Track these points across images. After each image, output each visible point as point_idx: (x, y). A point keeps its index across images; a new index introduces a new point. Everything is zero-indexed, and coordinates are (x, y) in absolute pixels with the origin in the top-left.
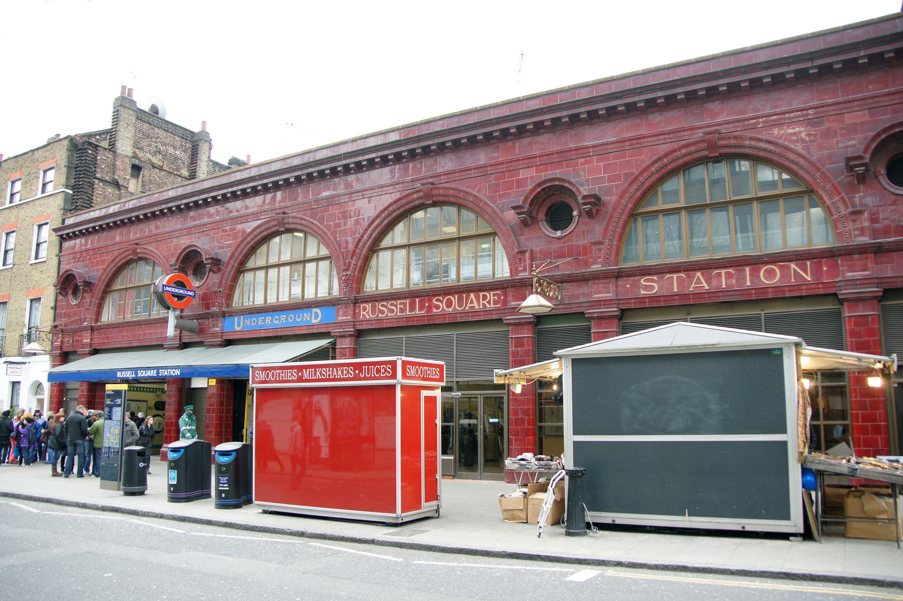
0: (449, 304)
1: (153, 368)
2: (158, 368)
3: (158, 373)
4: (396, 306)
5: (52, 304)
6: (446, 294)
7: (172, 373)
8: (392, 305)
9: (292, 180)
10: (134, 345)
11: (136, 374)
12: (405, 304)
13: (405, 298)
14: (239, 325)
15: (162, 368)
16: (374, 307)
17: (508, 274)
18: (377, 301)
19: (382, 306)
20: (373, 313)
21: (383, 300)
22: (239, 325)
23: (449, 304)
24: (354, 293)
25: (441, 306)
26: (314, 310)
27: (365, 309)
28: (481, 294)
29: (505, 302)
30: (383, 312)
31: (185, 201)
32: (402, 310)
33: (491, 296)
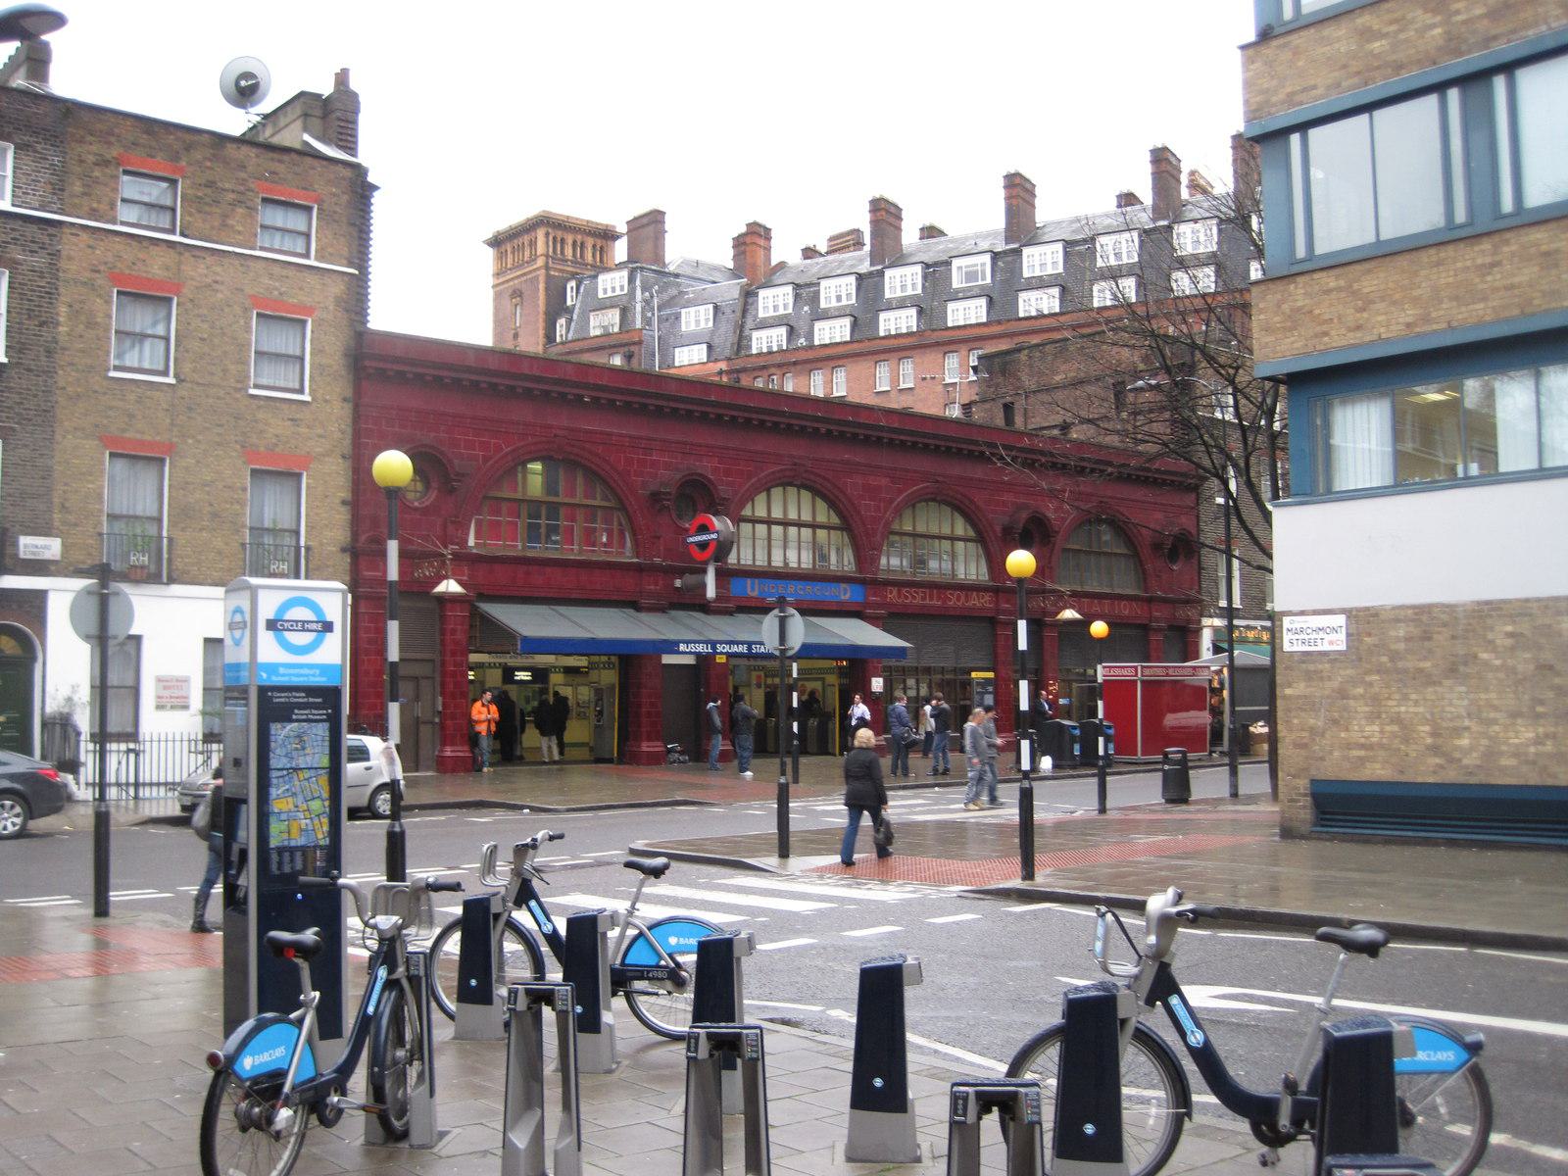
0: (958, 600)
1: (743, 643)
2: (750, 644)
3: (750, 648)
5: (346, 494)
11: (714, 648)
13: (926, 587)
14: (753, 589)
15: (756, 643)
16: (899, 592)
17: (987, 578)
20: (899, 597)
22: (753, 589)
23: (958, 600)
25: (954, 601)
26: (843, 586)
30: (907, 598)
32: (923, 599)
33: (987, 597)
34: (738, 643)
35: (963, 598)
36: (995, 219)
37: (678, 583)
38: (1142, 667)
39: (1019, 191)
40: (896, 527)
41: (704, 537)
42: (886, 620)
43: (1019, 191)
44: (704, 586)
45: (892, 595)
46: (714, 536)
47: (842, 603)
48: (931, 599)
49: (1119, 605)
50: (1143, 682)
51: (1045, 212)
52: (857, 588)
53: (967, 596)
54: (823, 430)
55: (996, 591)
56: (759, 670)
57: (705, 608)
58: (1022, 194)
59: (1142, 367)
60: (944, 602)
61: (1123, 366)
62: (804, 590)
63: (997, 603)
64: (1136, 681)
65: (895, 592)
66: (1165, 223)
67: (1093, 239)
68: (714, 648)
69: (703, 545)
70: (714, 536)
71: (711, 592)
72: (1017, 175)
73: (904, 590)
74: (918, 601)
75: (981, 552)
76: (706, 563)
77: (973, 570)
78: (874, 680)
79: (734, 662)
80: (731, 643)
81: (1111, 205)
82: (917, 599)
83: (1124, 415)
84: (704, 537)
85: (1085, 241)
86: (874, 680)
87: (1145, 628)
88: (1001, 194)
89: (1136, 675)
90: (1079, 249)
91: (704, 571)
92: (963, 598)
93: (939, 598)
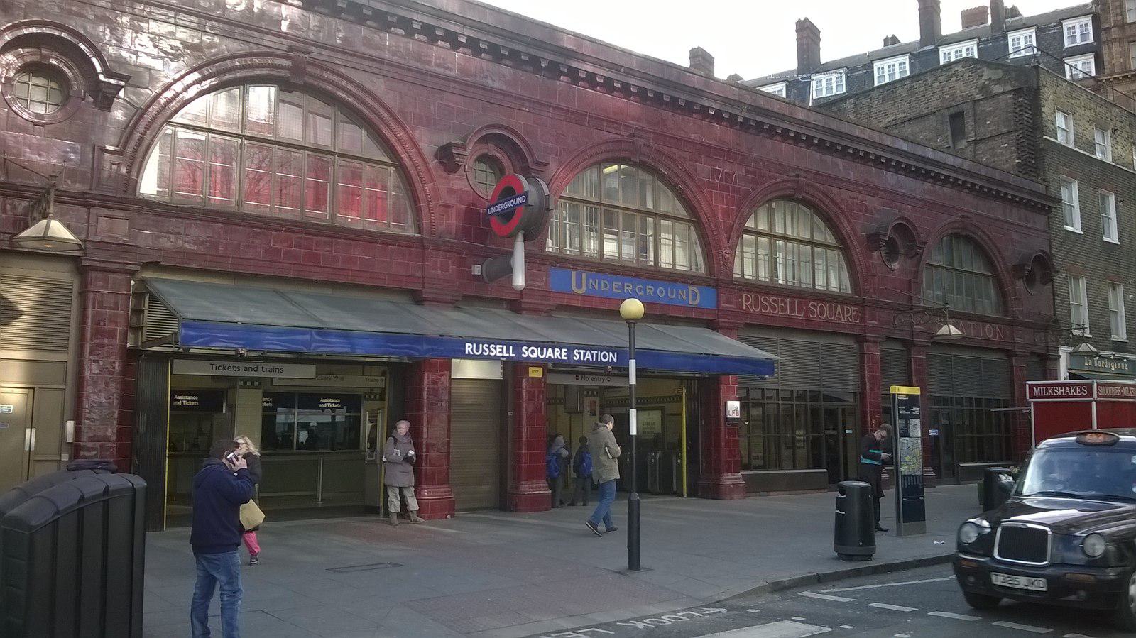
0: (822, 313)
3: (570, 354)
4: (777, 303)
6: (822, 301)
7: (600, 357)
8: (774, 301)
9: (544, 64)
10: (316, 277)
12: (786, 303)
16: (756, 298)
17: (848, 290)
18: (760, 293)
19: (765, 300)
21: (766, 294)
23: (822, 313)
24: (718, 277)
25: (818, 313)
26: (691, 288)
27: (747, 300)
28: (846, 307)
29: (863, 319)
31: (844, 143)
32: (784, 309)
33: (853, 311)
34: (553, 346)
35: (827, 312)
36: (789, 62)
37: (477, 270)
38: (1098, 384)
39: (807, 35)
40: (750, 224)
41: (509, 204)
42: (749, 327)
43: (807, 35)
44: (509, 271)
45: (748, 302)
46: (520, 200)
47: (691, 308)
48: (792, 310)
49: (984, 327)
50: (1097, 402)
51: (827, 54)
52: (711, 293)
53: (830, 307)
54: (666, 99)
55: (862, 304)
56: (593, 395)
57: (515, 304)
58: (811, 35)
59: (979, 97)
60: (806, 315)
61: (958, 99)
62: (645, 290)
63: (863, 319)
64: (1090, 403)
65: (752, 300)
66: (932, 47)
67: (871, 66)
68: (517, 349)
69: (507, 215)
70: (520, 200)
71: (519, 280)
72: (806, 20)
73: (761, 298)
74: (778, 311)
75: (843, 262)
76: (513, 237)
77: (834, 282)
78: (730, 403)
79: (554, 380)
80: (543, 345)
81: (880, 46)
82: (778, 308)
83: (962, 144)
84: (509, 204)
85: (864, 67)
86: (730, 403)
87: (1009, 354)
88: (794, 36)
89: (1090, 394)
90: (858, 69)
91: (510, 254)
92: (827, 312)
93: (800, 311)
